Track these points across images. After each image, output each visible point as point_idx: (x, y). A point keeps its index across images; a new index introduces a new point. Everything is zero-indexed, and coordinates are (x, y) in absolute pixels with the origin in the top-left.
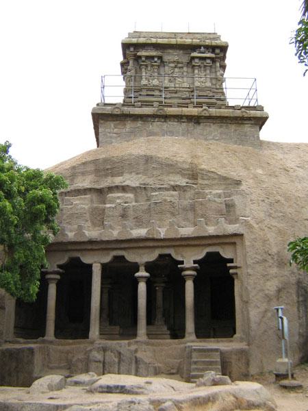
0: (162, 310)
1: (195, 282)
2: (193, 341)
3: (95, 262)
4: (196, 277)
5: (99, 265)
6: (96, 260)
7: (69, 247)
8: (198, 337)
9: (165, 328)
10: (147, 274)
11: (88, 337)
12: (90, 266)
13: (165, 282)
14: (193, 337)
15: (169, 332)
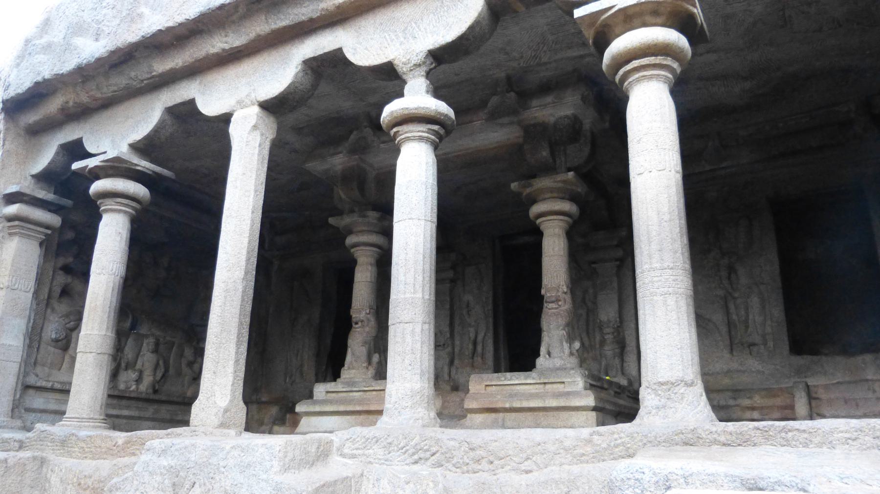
0: (566, 306)
1: (678, 90)
2: (689, 441)
3: (241, 104)
4: (691, 63)
5: (256, 109)
6: (243, 91)
7: (163, 65)
8: (724, 410)
9: (577, 382)
10: (442, 107)
11: (186, 423)
12: (225, 119)
13: (573, 198)
14: (694, 409)
15: (590, 400)
